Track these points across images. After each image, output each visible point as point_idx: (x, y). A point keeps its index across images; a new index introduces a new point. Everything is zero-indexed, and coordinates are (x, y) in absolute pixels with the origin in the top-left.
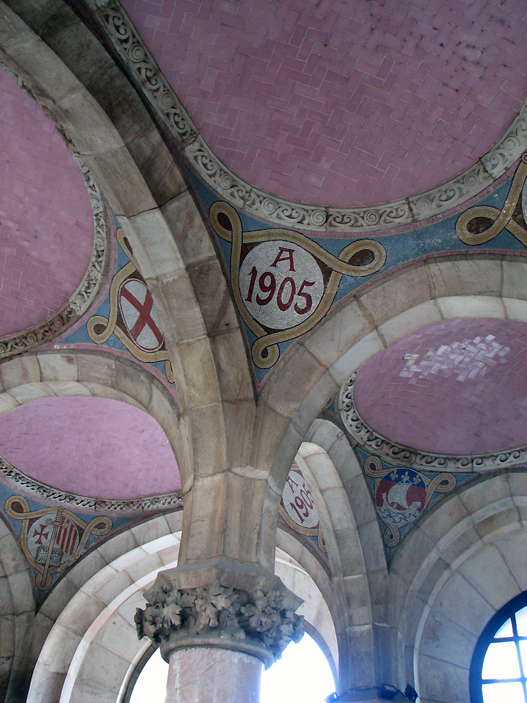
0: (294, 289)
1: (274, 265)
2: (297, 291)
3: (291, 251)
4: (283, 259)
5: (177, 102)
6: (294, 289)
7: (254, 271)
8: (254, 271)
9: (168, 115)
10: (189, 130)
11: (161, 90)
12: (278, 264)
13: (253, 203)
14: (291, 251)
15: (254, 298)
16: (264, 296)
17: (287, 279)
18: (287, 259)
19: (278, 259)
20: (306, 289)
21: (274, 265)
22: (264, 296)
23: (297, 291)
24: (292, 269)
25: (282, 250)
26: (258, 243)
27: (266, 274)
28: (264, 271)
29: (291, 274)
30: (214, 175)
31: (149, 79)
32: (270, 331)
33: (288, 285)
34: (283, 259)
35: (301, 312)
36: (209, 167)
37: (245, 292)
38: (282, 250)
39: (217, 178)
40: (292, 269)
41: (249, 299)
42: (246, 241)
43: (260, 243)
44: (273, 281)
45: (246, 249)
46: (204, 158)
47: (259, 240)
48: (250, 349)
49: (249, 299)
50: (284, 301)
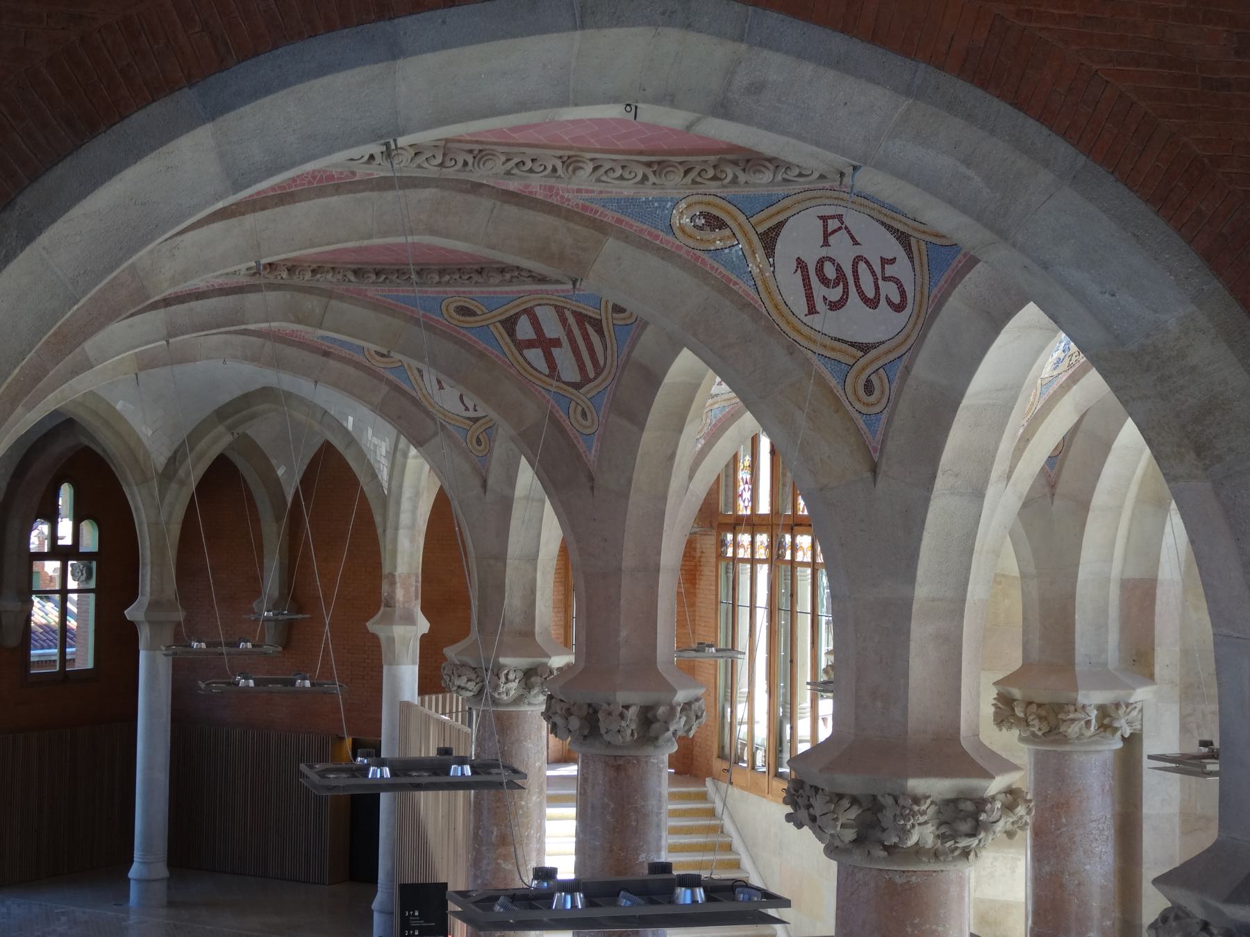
0: (873, 273)
1: (826, 243)
2: (879, 276)
3: (840, 217)
4: (834, 232)
5: (506, 149)
6: (873, 273)
7: (801, 265)
8: (801, 266)
9: (508, 173)
10: (559, 164)
11: (470, 160)
12: (831, 239)
13: (735, 177)
14: (840, 217)
15: (820, 305)
16: (835, 294)
17: (858, 259)
18: (840, 228)
19: (826, 235)
20: (890, 272)
21: (826, 243)
22: (835, 294)
23: (879, 276)
24: (856, 243)
25: (824, 219)
26: (781, 225)
27: (821, 262)
28: (817, 258)
29: (857, 251)
30: (645, 178)
31: (441, 165)
32: (865, 348)
33: (862, 266)
34: (834, 232)
35: (899, 308)
36: (626, 175)
37: (800, 306)
38: (824, 219)
39: (652, 179)
40: (856, 243)
41: (812, 310)
42: (760, 230)
43: (786, 220)
44: (839, 269)
45: (769, 240)
46: (611, 174)
47: (780, 218)
48: (839, 392)
49: (812, 310)
50: (870, 294)
